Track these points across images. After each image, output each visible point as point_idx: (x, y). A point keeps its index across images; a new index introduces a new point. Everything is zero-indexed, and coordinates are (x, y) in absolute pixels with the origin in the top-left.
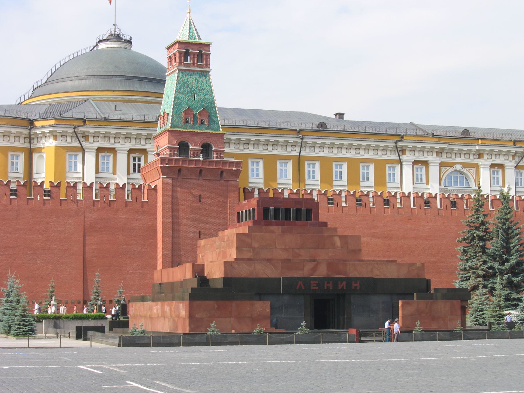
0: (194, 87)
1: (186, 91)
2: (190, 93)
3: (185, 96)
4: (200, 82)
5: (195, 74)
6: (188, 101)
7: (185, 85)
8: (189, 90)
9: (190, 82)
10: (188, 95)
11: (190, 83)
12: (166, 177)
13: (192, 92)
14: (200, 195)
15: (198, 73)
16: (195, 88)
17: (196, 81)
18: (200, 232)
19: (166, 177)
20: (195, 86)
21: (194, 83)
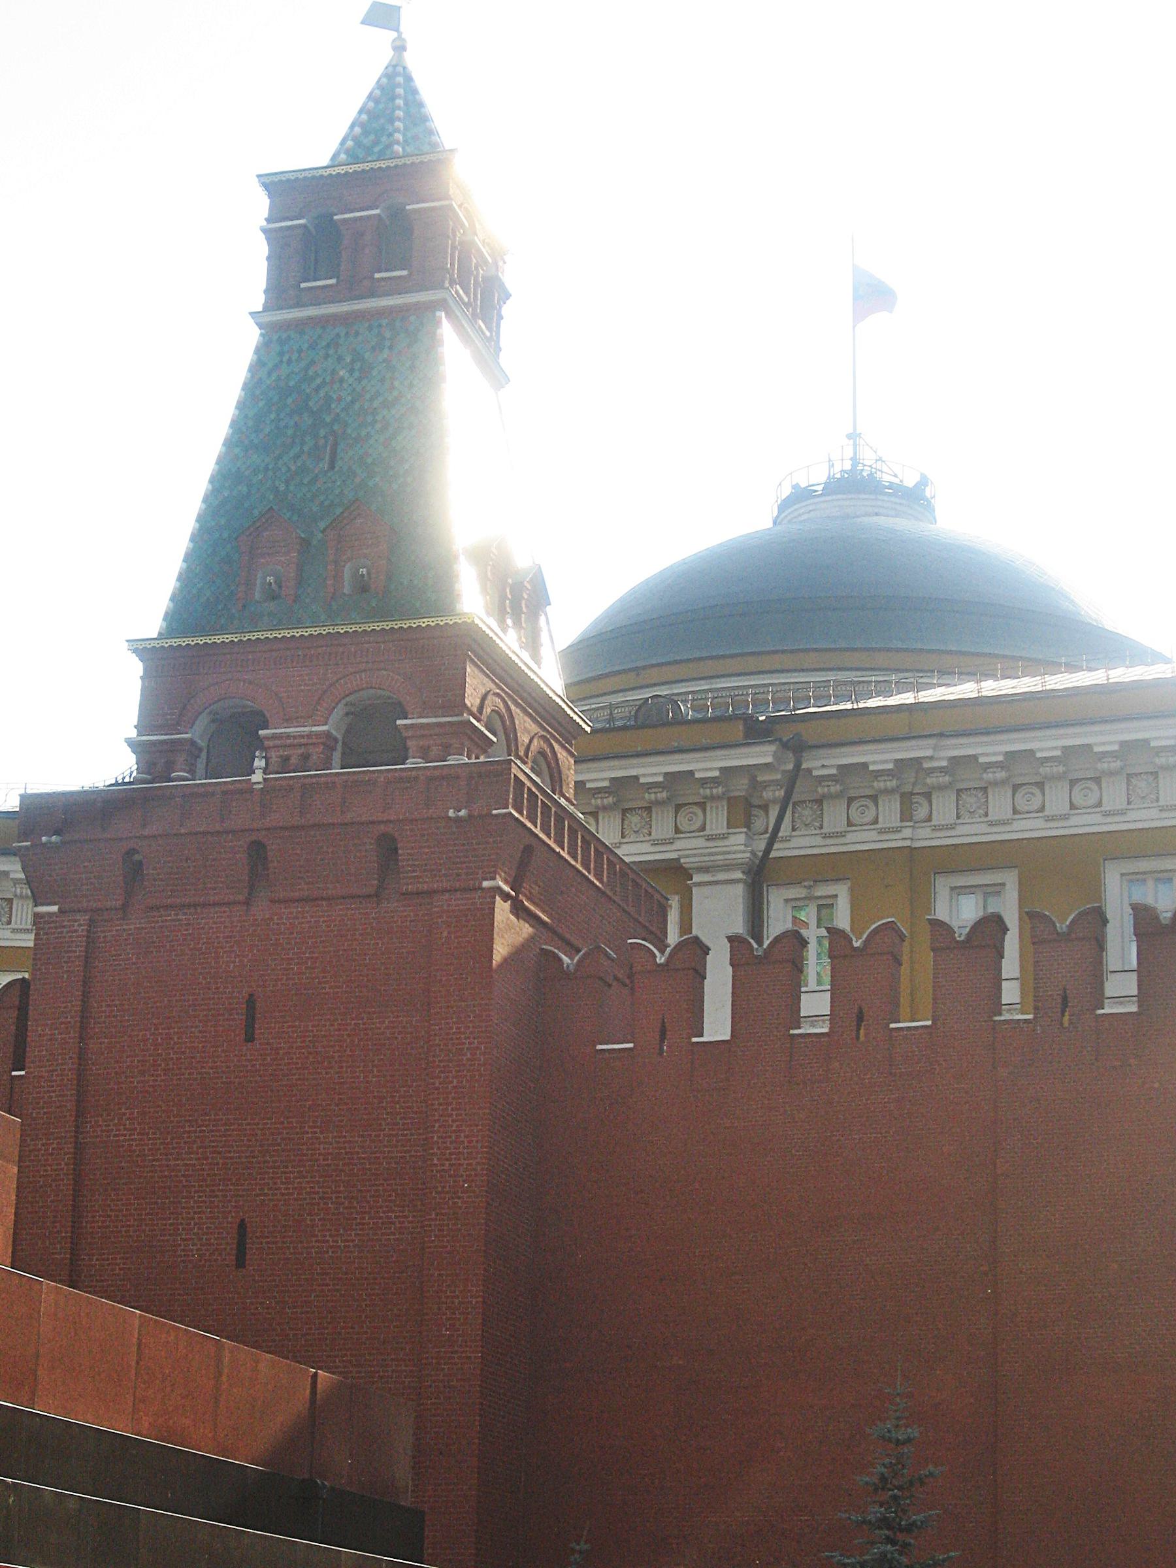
0: (339, 399)
1: (290, 432)
2: (308, 439)
3: (279, 457)
4: (374, 373)
5: (357, 334)
6: (287, 482)
7: (290, 400)
8: (307, 420)
9: (319, 381)
10: (296, 449)
11: (317, 390)
12: (55, 909)
13: (322, 432)
14: (251, 1001)
15: (370, 328)
16: (343, 404)
17: (351, 371)
18: (242, 1225)
19: (55, 909)
20: (344, 394)
21: (342, 380)
